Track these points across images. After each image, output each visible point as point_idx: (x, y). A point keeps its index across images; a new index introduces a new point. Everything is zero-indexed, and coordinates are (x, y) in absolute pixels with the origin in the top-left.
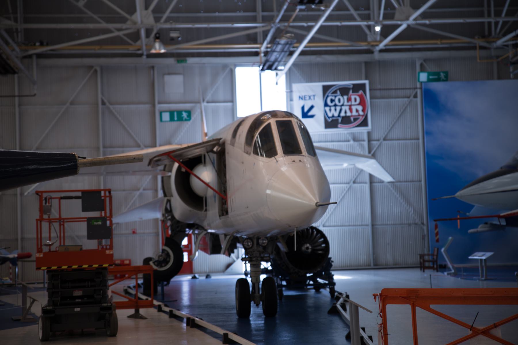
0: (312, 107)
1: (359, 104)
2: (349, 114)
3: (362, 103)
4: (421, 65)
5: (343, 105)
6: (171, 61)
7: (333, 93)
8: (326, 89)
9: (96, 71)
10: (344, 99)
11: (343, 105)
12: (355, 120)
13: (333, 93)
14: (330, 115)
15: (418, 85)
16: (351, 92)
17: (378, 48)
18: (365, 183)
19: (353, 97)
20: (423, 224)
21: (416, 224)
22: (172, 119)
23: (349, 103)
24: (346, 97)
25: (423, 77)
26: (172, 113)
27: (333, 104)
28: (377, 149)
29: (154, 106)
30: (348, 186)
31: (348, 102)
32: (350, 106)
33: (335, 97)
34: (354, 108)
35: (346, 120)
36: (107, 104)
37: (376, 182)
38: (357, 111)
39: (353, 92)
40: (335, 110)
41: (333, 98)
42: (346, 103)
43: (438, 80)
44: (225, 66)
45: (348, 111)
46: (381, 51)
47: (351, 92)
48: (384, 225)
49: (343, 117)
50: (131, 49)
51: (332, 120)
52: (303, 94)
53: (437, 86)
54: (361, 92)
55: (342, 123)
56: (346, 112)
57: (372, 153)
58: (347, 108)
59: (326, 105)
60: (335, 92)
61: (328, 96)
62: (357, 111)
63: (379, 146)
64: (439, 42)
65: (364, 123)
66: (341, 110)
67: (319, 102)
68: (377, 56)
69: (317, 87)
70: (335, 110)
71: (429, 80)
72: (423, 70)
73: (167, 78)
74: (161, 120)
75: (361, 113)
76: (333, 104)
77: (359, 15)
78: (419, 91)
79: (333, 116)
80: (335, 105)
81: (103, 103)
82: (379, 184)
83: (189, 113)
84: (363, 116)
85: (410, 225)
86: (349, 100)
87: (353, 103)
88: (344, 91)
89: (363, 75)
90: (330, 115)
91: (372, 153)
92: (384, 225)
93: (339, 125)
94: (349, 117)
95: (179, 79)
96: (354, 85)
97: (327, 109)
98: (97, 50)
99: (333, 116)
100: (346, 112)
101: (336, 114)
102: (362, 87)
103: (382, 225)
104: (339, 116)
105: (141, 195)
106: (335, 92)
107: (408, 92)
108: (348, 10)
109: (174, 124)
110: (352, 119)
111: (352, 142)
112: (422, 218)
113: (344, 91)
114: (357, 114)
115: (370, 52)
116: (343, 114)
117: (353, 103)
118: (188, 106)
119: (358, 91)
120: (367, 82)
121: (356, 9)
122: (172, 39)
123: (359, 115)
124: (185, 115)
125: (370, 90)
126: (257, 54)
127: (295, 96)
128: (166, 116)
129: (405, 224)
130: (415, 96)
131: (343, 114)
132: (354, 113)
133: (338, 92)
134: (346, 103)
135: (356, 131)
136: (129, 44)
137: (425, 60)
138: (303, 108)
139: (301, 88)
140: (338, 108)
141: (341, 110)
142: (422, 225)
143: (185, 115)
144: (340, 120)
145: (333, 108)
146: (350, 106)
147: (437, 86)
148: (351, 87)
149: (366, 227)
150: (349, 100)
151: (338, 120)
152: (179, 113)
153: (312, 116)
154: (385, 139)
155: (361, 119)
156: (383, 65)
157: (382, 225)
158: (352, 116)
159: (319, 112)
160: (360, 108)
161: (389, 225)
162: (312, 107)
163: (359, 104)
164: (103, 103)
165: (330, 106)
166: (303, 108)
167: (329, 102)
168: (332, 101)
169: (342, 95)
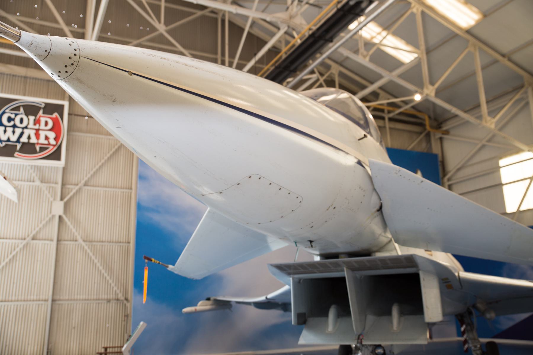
1: (51, 130)
2: (33, 140)
3: (56, 128)
5: (26, 127)
7: (11, 110)
10: (29, 119)
11: (26, 127)
12: (42, 149)
13: (11, 110)
16: (41, 112)
18: (52, 240)
19: (43, 120)
20: (127, 299)
21: (118, 300)
23: (37, 127)
24: (32, 118)
27: (12, 123)
28: (74, 195)
30: (24, 242)
31: (35, 124)
32: (37, 130)
33: (16, 115)
34: (42, 134)
35: (28, 149)
37: (65, 240)
38: (47, 138)
39: (44, 113)
40: (14, 132)
41: (13, 116)
42: (31, 125)
47: (41, 112)
48: (71, 300)
49: (24, 144)
51: (6, 145)
54: (56, 115)
55: (21, 151)
56: (29, 138)
57: (66, 200)
58: (33, 133)
60: (17, 109)
61: (4, 113)
62: (47, 138)
63: (79, 191)
65: (56, 156)
70: (14, 132)
75: (53, 142)
76: (12, 123)
77: (72, 32)
79: (8, 140)
80: (14, 126)
82: (72, 243)
84: (54, 146)
85: (109, 301)
86: (37, 122)
87: (42, 126)
88: (31, 110)
91: (66, 200)
92: (71, 300)
93: (16, 154)
94: (33, 144)
96: (47, 104)
99: (8, 140)
100: (29, 138)
101: (14, 138)
102: (59, 109)
103: (68, 300)
104: (18, 141)
106: (17, 109)
108: (57, 22)
110: (38, 148)
111: (38, 183)
112: (126, 292)
113: (31, 110)
114: (46, 142)
116: (24, 139)
117: (42, 126)
119: (52, 114)
121: (68, 24)
123: (49, 144)
125: (70, 114)
129: (102, 300)
131: (24, 139)
132: (42, 140)
133: (22, 109)
134: (31, 125)
135: (42, 165)
140: (18, 131)
142: (125, 302)
144: (19, 146)
145: (10, 130)
146: (37, 130)
148: (43, 105)
149: (43, 302)
150: (37, 122)
151: (16, 146)
154: (86, 185)
157: (68, 300)
158: (38, 144)
161: (80, 300)
163: (51, 130)
165: (6, 127)
168: (10, 119)
169: (27, 115)
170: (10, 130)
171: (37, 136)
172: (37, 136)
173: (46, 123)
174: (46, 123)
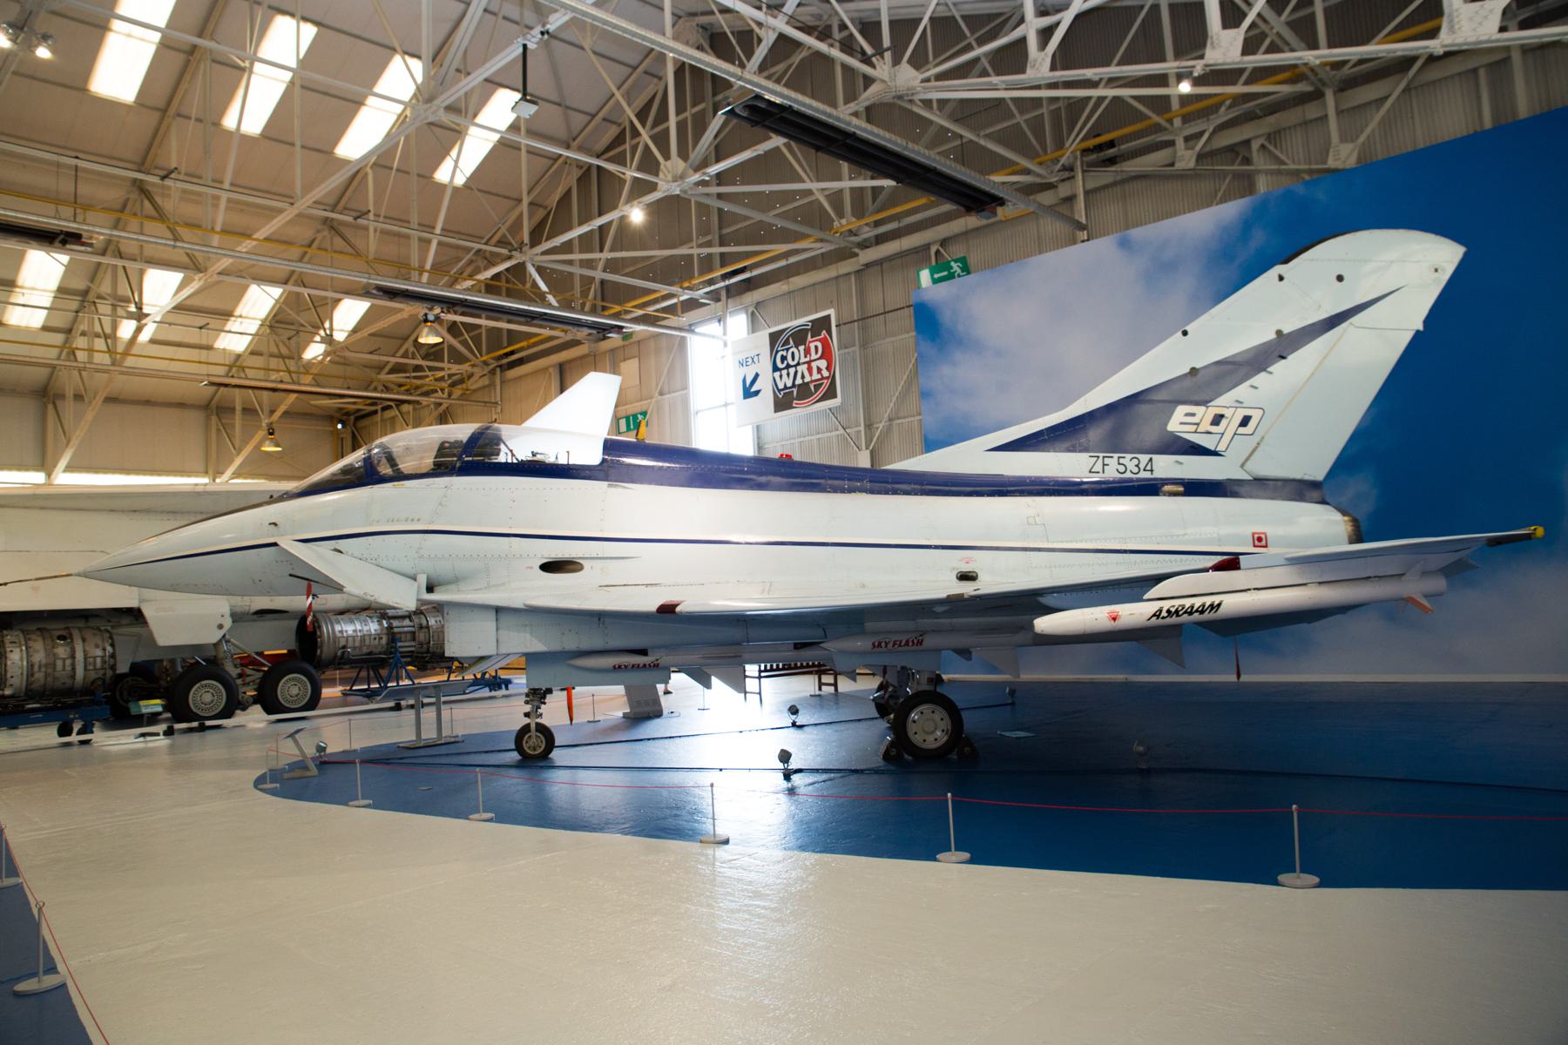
0: (757, 375)
2: (807, 379)
3: (827, 354)
4: (937, 252)
8: (774, 337)
12: (817, 387)
14: (781, 386)
19: (812, 346)
24: (802, 348)
34: (814, 365)
38: (819, 370)
45: (806, 374)
55: (799, 398)
59: (775, 369)
60: (787, 343)
62: (819, 370)
65: (831, 393)
68: (867, 256)
75: (825, 373)
80: (788, 366)
86: (807, 352)
88: (799, 337)
97: (777, 374)
101: (789, 384)
104: (794, 385)
120: (831, 312)
131: (799, 381)
132: (816, 376)
137: (944, 242)
140: (792, 371)
145: (784, 372)
150: (807, 352)
153: (757, 393)
159: (765, 385)
160: (823, 364)
162: (757, 375)
167: (780, 365)
168: (784, 358)
171: (810, 370)
172: (810, 370)
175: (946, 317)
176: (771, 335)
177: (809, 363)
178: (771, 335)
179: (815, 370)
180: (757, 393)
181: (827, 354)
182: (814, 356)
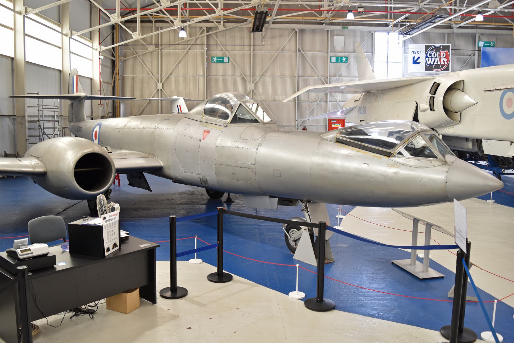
0: (419, 58)
2: (439, 63)
3: (447, 57)
4: (479, 37)
6: (338, 27)
8: (427, 47)
9: (296, 32)
12: (442, 66)
14: (429, 63)
15: (477, 49)
17: (458, 26)
19: (442, 53)
22: (337, 61)
24: (438, 53)
25: (481, 44)
26: (337, 58)
29: (327, 53)
34: (442, 60)
35: (437, 67)
36: (302, 51)
43: (489, 46)
44: (369, 32)
45: (439, 61)
46: (459, 28)
50: (319, 19)
52: (414, 50)
53: (488, 49)
56: (437, 62)
59: (427, 57)
60: (432, 50)
64: (493, 24)
66: (435, 60)
67: (423, 55)
68: (456, 30)
69: (422, 47)
71: (484, 46)
72: (480, 40)
73: (335, 37)
74: (331, 62)
75: (446, 63)
78: (476, 52)
80: (432, 58)
81: (299, 51)
83: (347, 58)
86: (440, 55)
88: (437, 49)
89: (446, 41)
90: (429, 63)
95: (343, 38)
97: (427, 59)
98: (300, 19)
100: (437, 62)
101: (432, 63)
104: (433, 64)
105: (318, 104)
106: (432, 50)
107: (470, 52)
109: (338, 64)
115: (451, 28)
116: (435, 63)
118: (346, 54)
120: (450, 45)
122: (359, 12)
124: (344, 59)
126: (387, 25)
127: (410, 51)
128: (334, 60)
130: (474, 55)
131: (435, 63)
132: (442, 63)
134: (438, 57)
136: (318, 17)
137: (481, 34)
138: (414, 58)
139: (412, 47)
140: (433, 59)
141: (435, 60)
143: (344, 59)
145: (430, 59)
147: (488, 49)
150: (440, 55)
152: (341, 58)
153: (419, 63)
155: (446, 66)
156: (457, 35)
159: (422, 61)
160: (445, 60)
162: (419, 58)
164: (299, 51)
166: (414, 58)
168: (430, 55)
170: (430, 59)
173: (443, 55)
174: (443, 55)
175: (492, 57)
176: (426, 46)
177: (440, 58)
178: (426, 46)
179: (442, 61)
180: (419, 63)
181: (447, 57)
182: (442, 57)
